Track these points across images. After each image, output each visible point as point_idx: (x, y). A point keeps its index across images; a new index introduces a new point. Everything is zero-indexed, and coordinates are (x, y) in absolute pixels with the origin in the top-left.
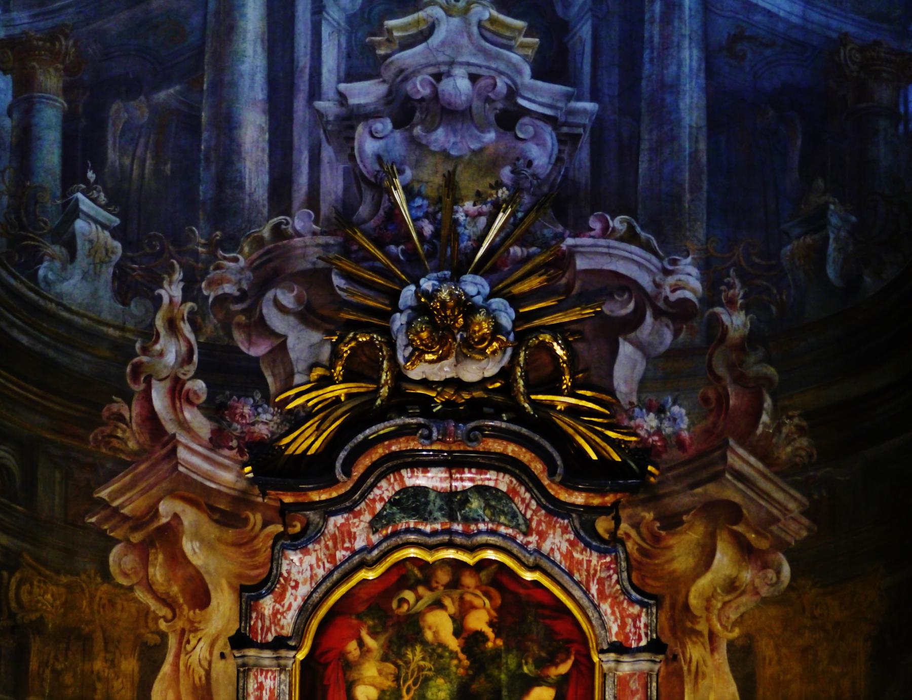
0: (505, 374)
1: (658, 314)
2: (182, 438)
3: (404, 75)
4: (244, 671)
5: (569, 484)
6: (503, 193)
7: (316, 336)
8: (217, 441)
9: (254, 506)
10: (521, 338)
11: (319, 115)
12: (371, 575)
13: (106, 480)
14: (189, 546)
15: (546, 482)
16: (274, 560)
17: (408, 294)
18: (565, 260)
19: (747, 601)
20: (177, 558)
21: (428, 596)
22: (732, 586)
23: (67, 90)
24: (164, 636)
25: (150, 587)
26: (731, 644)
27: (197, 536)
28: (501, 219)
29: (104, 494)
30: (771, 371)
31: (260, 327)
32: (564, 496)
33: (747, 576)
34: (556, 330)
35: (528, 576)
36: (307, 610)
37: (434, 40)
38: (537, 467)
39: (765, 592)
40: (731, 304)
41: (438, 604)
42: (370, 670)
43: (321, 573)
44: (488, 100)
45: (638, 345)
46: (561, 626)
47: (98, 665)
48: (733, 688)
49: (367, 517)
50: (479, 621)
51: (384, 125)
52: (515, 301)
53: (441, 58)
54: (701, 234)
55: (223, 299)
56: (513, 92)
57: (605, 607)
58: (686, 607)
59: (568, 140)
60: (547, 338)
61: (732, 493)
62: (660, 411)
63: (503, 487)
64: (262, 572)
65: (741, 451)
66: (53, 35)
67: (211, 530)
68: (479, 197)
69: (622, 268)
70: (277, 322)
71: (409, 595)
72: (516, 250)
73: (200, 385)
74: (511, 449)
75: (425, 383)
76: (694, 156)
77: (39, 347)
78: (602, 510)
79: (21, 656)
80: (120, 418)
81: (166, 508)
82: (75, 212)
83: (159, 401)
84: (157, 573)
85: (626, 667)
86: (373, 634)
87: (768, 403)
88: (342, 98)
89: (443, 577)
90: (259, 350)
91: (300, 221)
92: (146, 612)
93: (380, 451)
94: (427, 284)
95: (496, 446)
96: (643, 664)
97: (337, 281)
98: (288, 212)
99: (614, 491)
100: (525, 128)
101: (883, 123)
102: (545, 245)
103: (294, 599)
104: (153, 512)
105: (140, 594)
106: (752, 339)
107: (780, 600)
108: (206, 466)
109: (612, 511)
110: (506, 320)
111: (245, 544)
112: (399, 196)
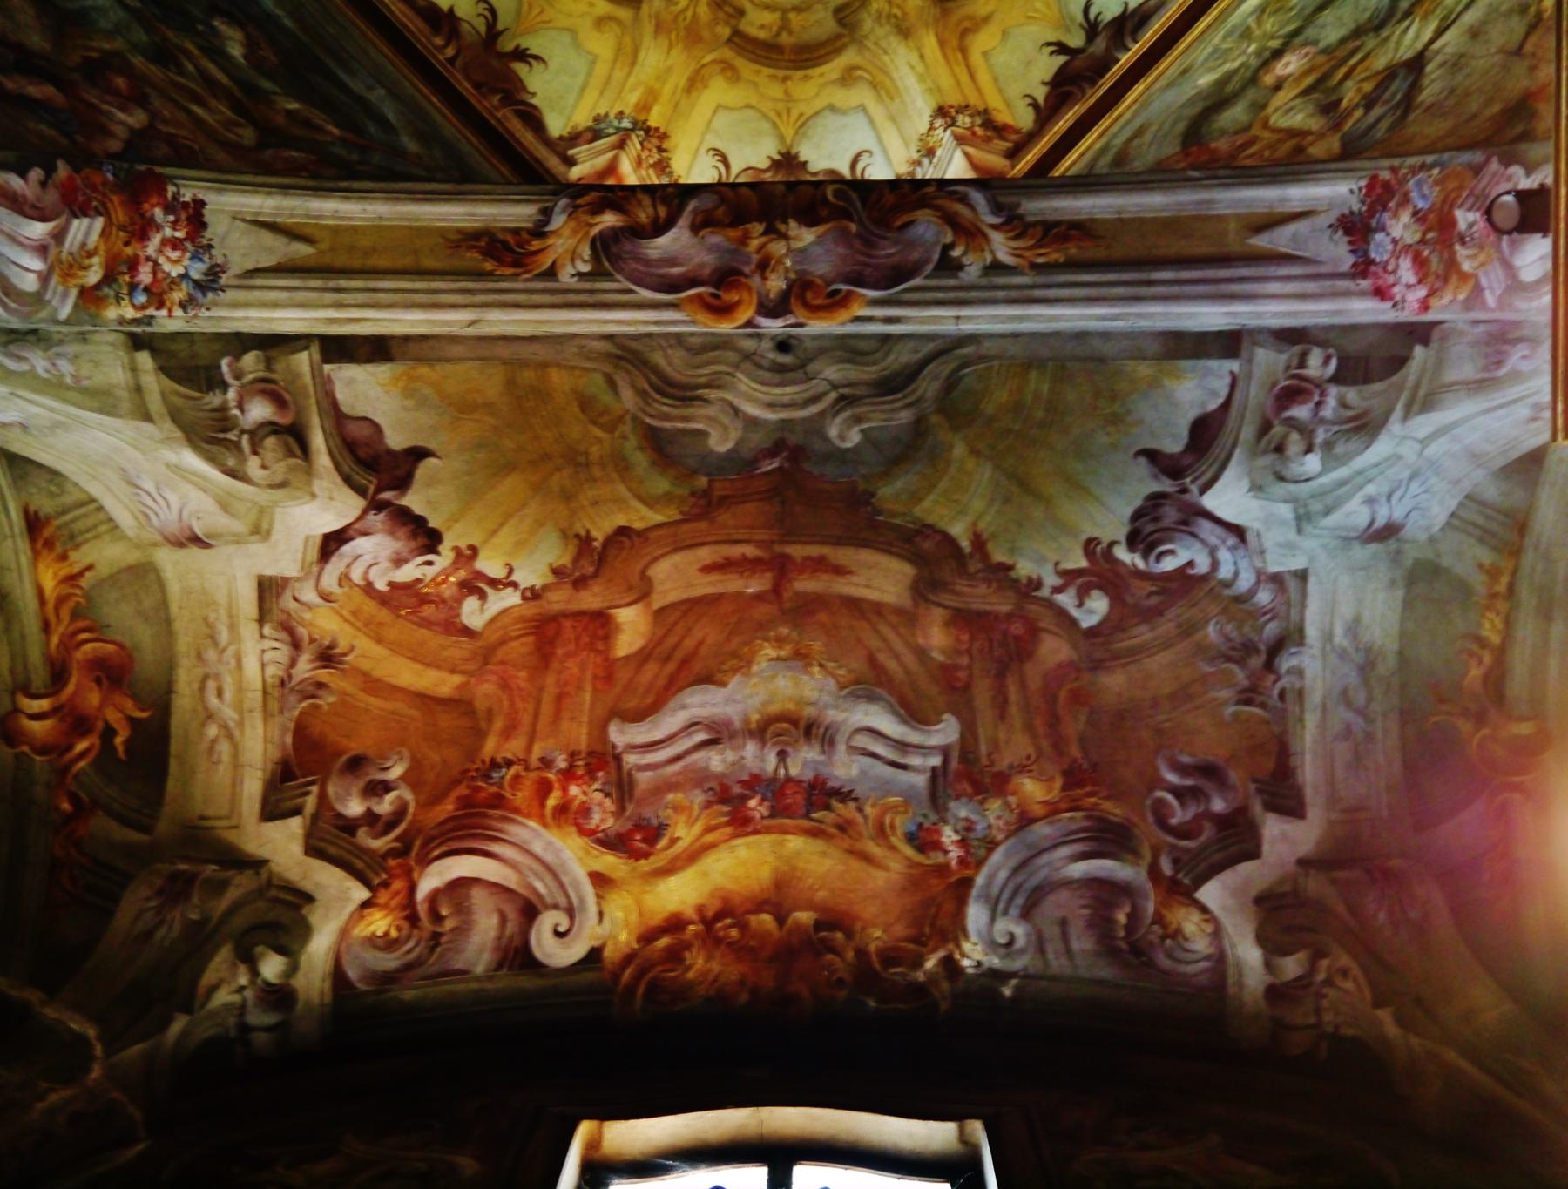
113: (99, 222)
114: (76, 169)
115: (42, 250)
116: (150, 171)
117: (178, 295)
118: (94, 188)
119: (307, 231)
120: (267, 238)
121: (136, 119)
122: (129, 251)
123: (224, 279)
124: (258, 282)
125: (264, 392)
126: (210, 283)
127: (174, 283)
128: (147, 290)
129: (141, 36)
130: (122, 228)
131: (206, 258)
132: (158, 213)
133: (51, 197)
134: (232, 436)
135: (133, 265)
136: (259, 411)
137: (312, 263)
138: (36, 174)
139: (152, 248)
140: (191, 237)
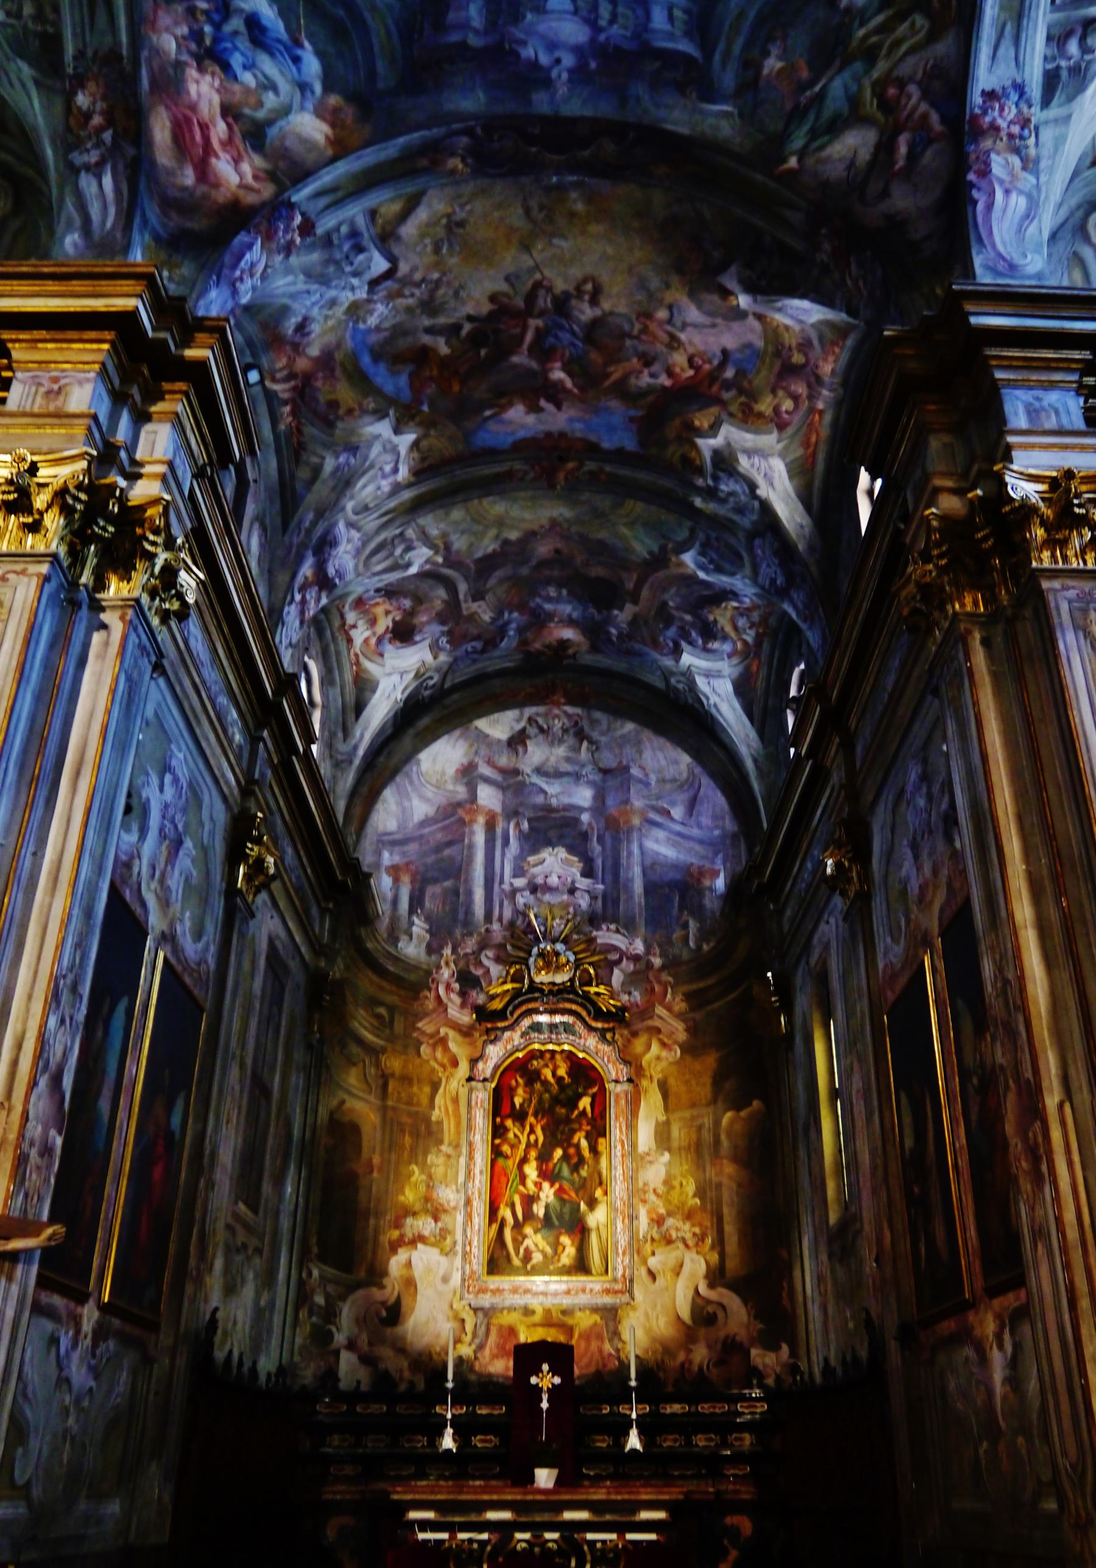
0: (572, 980)
1: (628, 958)
2: (450, 1005)
3: (534, 876)
4: (471, 1091)
5: (596, 1019)
6: (570, 916)
7: (500, 967)
8: (463, 1005)
9: (476, 1029)
10: (577, 968)
11: (503, 890)
12: (520, 1055)
13: (421, 1019)
14: (452, 1045)
15: (587, 1019)
16: (483, 1049)
17: (535, 950)
18: (591, 941)
19: (664, 1064)
20: (446, 1049)
21: (542, 1062)
22: (658, 1058)
23: (412, 882)
24: (440, 1079)
25: (436, 1060)
26: (658, 1081)
27: (455, 1040)
28: (570, 925)
29: (420, 1025)
30: (670, 979)
31: (480, 964)
32: (594, 1024)
33: (664, 1054)
34: (590, 964)
35: (581, 1055)
36: (496, 1068)
37: (545, 864)
38: (584, 1014)
39: (671, 1060)
40: (655, 955)
41: (546, 1066)
42: (520, 1091)
43: (501, 1054)
44: (564, 884)
45: (622, 970)
46: (592, 1074)
47: (415, 1089)
48: (660, 1097)
49: (519, 1033)
50: (562, 1072)
51: (527, 893)
52: (575, 953)
53: (548, 870)
54: (642, 930)
55: (466, 955)
56: (573, 882)
57: (610, 1066)
58: (641, 1066)
59: (594, 898)
60: (586, 966)
61: (657, 1023)
62: (630, 993)
63: (571, 1021)
64: (478, 1054)
65: (660, 1008)
66: (407, 864)
67: (459, 1038)
68: (561, 918)
69: (614, 942)
70: (486, 962)
71: (535, 1063)
72: (575, 937)
73: (456, 986)
74: (574, 1007)
75: (542, 983)
76: (640, 904)
77: (397, 972)
78: (608, 1030)
79: (385, 1086)
80: (427, 997)
81: (443, 1031)
82: (411, 924)
83: (442, 991)
84: (439, 1054)
85: (619, 1088)
86: (521, 1077)
87: (670, 990)
88: (512, 884)
89: (548, 1056)
90: (479, 972)
91: (496, 926)
92: (433, 1070)
93: (524, 1008)
94: (542, 946)
95: (568, 1006)
96: (626, 1087)
97: (509, 947)
98: (491, 923)
99: (613, 1021)
100: (578, 894)
101: (707, 893)
102: (585, 934)
103: (491, 1064)
104: (438, 1032)
105: (433, 1063)
106: (663, 968)
107: (677, 1063)
108: (458, 1015)
109: (612, 1030)
110: (572, 958)
111: (472, 1044)
112: (532, 916)
113: (993, 156)
114: (969, 168)
115: (1007, 192)
116: (969, 122)
117: (1025, 109)
118: (978, 158)
119: (1000, 24)
120: (1001, 51)
121: (913, 89)
122: (1005, 139)
123: (1019, 80)
124: (1021, 58)
125: (1065, 43)
126: (1020, 89)
127: (1020, 112)
128: (1022, 128)
129: (858, 66)
130: (995, 142)
131: (1009, 90)
132: (988, 119)
133: (983, 184)
134: (1083, 66)
135: (1011, 136)
136: (1073, 47)
137: (1015, 25)
138: (975, 194)
139: (1002, 124)
140: (999, 100)
